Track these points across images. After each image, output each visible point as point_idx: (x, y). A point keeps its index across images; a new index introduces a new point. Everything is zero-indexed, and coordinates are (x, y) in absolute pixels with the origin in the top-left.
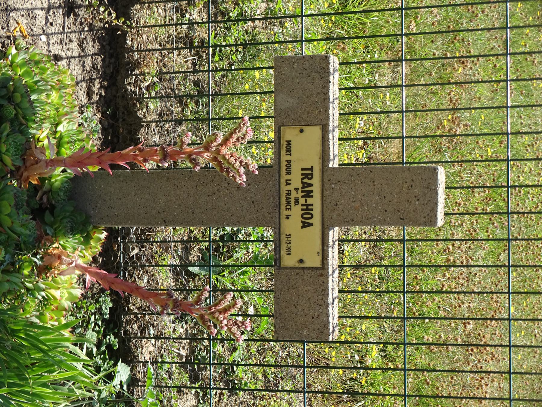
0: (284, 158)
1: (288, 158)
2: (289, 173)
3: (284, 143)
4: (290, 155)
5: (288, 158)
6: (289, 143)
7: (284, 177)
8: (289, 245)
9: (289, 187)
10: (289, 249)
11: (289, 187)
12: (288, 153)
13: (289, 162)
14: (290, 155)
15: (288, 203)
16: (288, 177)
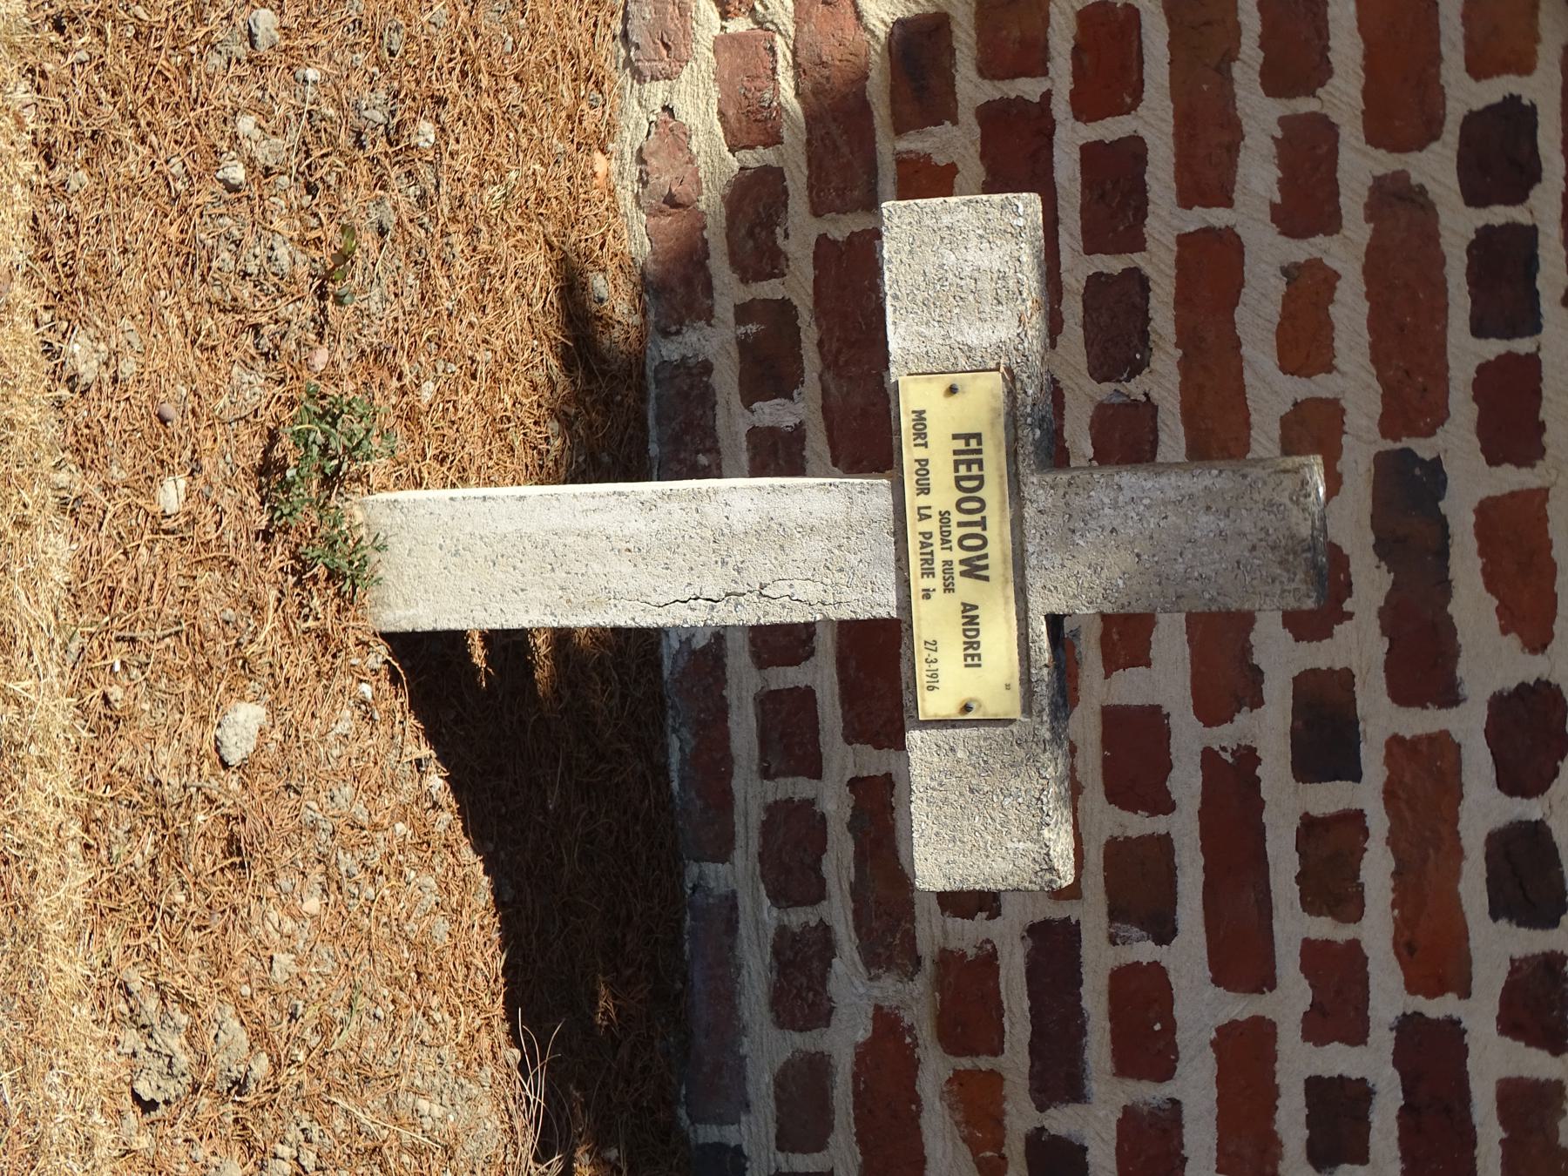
0: (910, 454)
1: (920, 453)
2: (924, 490)
3: (906, 422)
4: (926, 445)
5: (920, 453)
6: (920, 416)
7: (912, 500)
8: (934, 666)
9: (925, 526)
10: (934, 675)
11: (925, 526)
12: (919, 441)
13: (922, 463)
14: (926, 445)
15: (928, 561)
16: (923, 500)
